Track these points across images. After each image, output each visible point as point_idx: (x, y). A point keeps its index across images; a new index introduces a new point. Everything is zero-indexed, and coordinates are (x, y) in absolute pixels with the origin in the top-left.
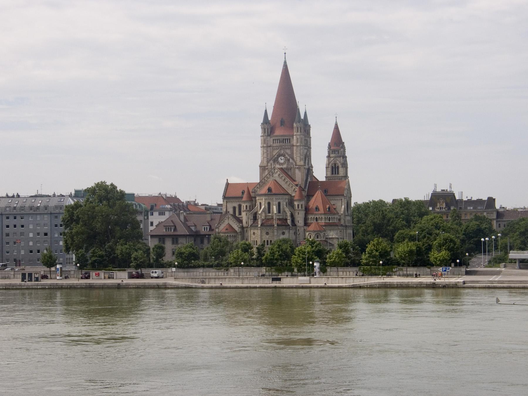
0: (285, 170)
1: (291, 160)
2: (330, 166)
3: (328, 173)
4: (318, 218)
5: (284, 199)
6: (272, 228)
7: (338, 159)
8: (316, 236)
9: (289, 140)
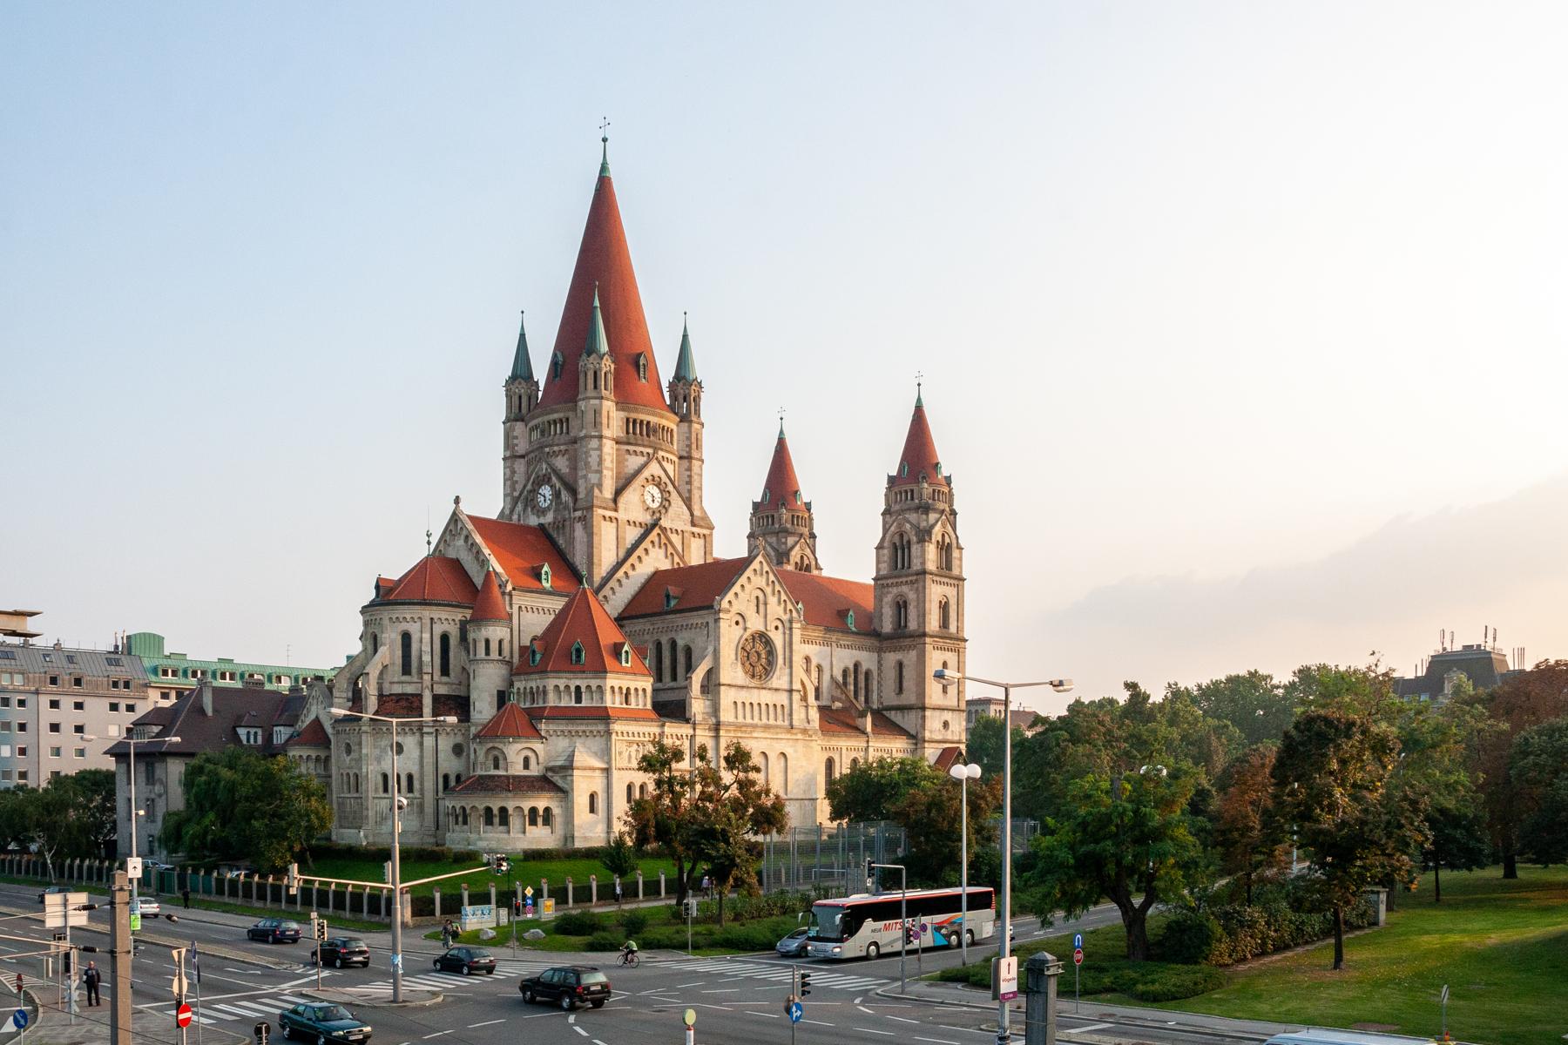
0: (551, 531)
1: (565, 496)
2: (886, 544)
3: (880, 566)
4: (535, 690)
5: (429, 622)
6: (357, 729)
7: (913, 517)
8: (491, 757)
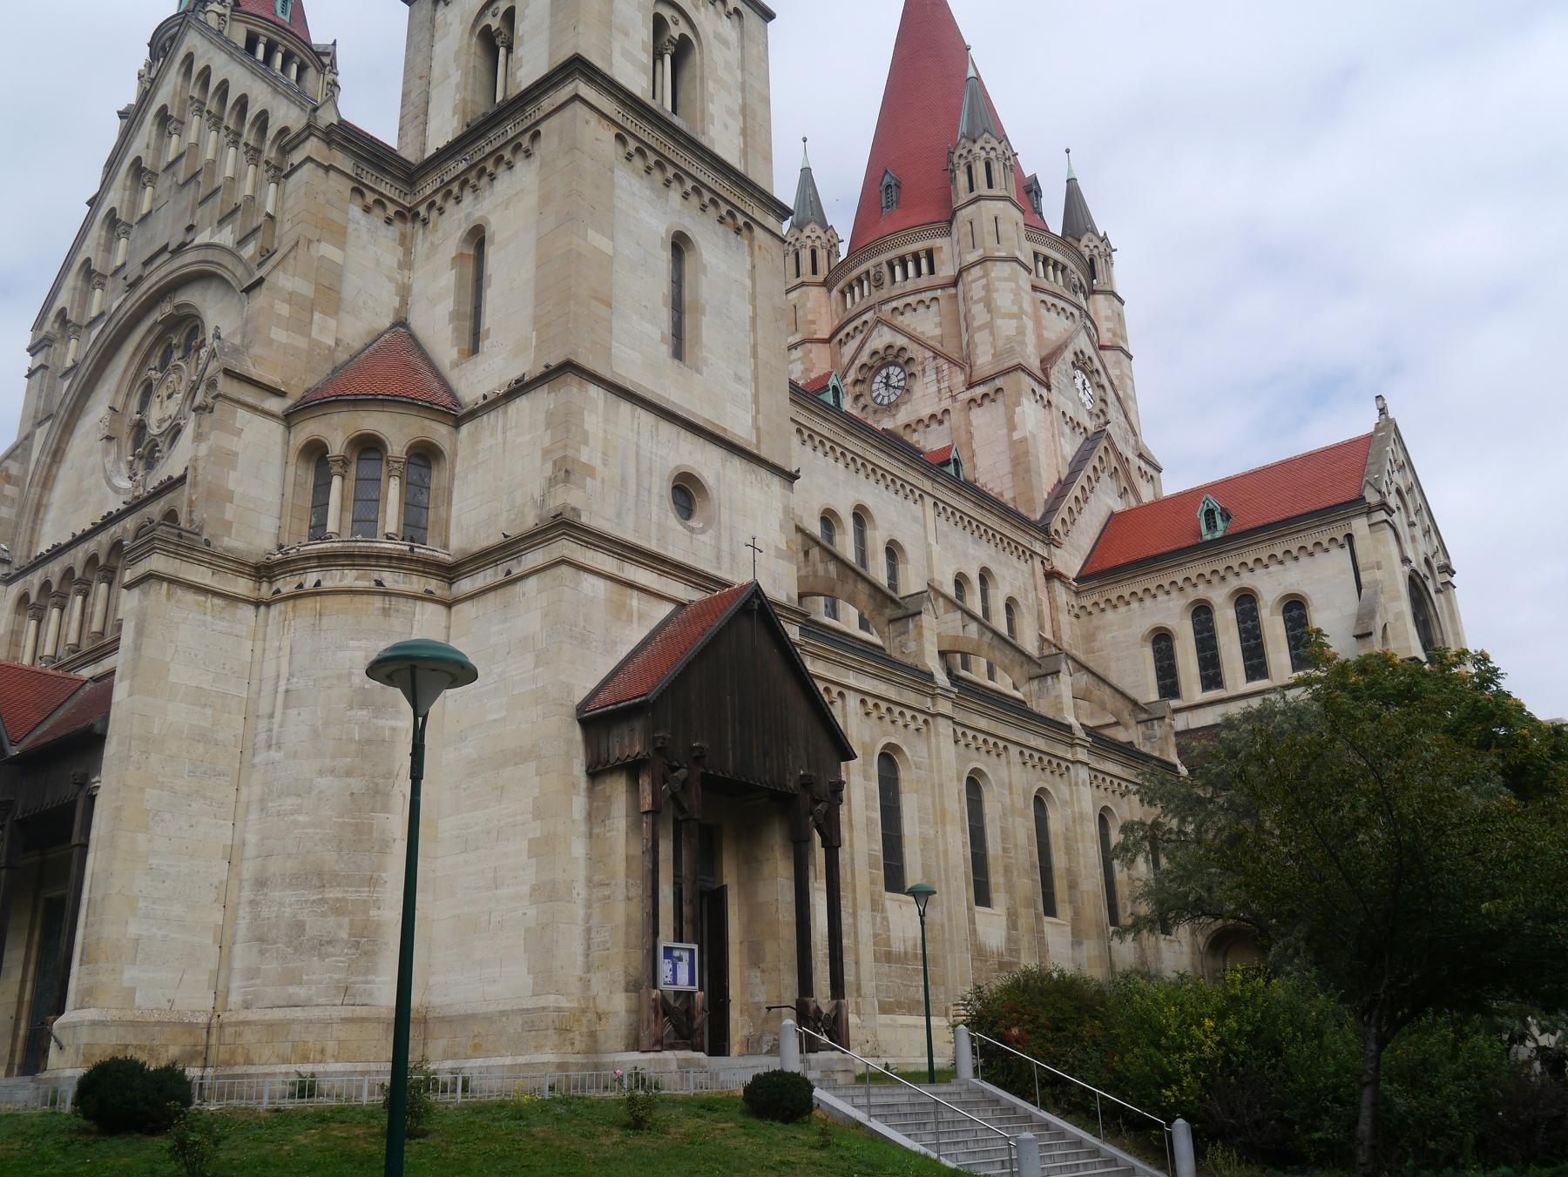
9: (924, 263)
